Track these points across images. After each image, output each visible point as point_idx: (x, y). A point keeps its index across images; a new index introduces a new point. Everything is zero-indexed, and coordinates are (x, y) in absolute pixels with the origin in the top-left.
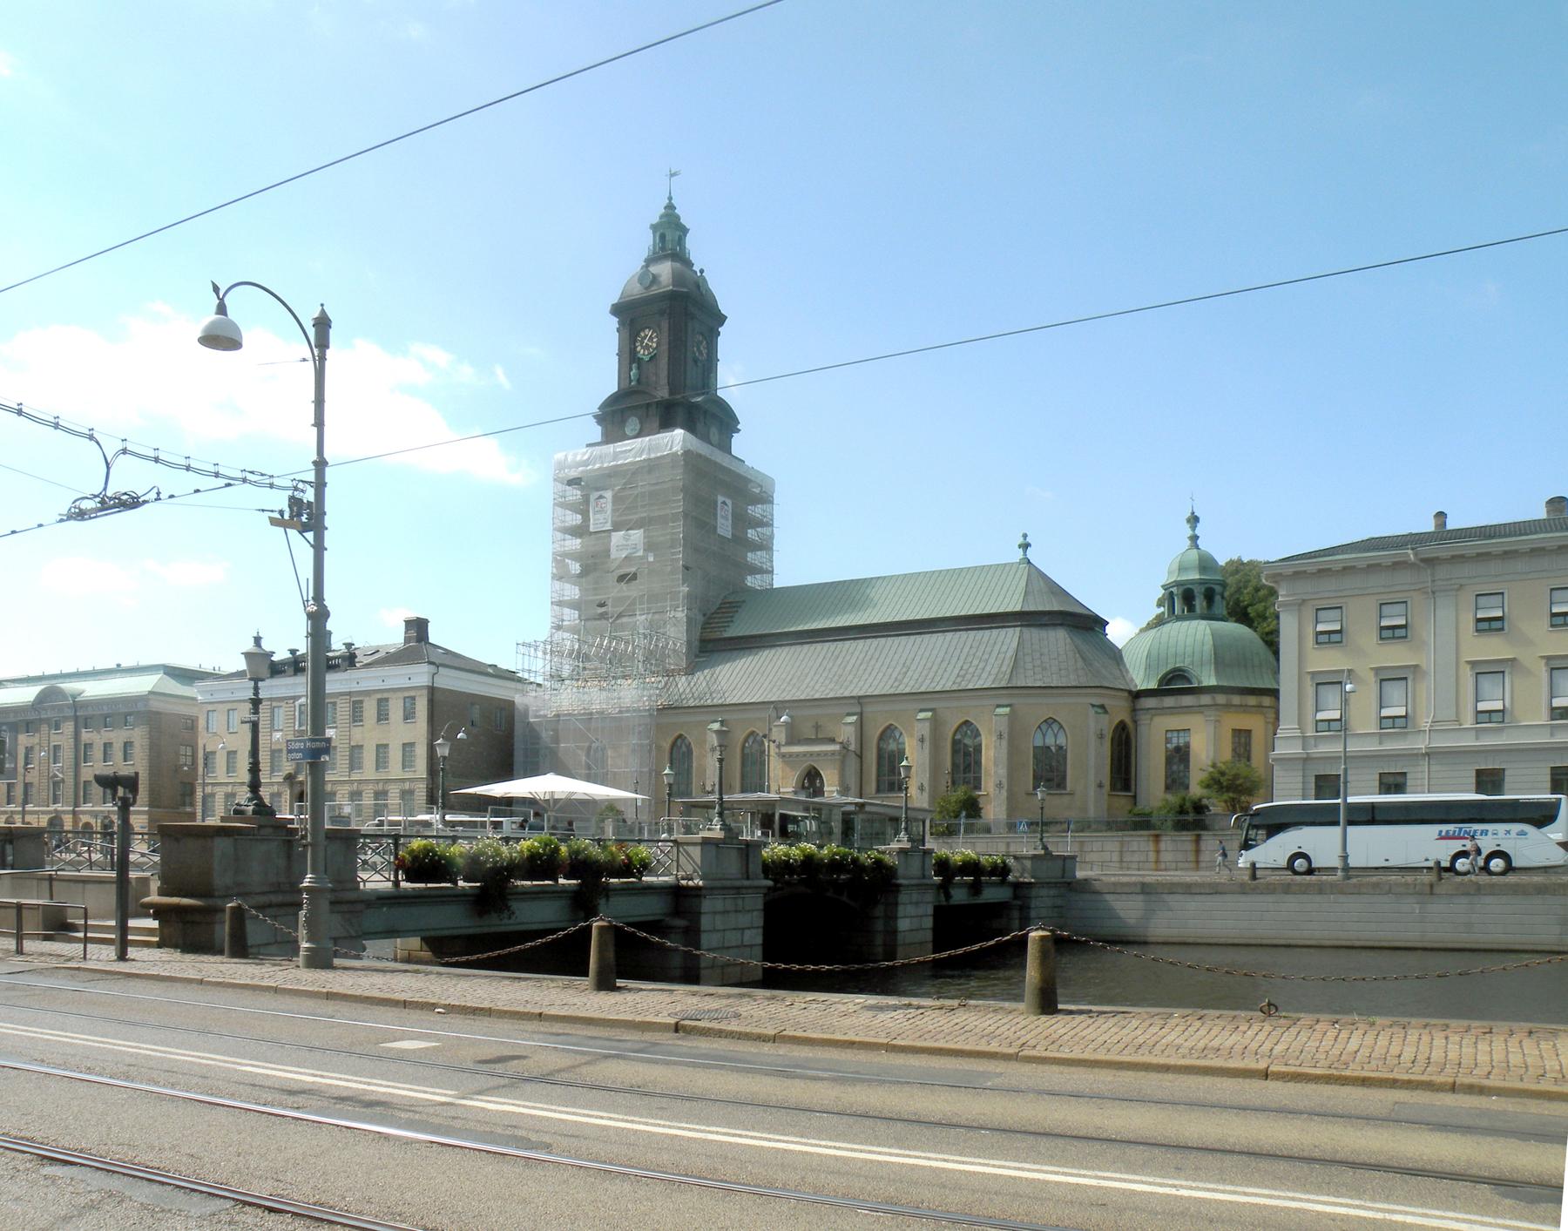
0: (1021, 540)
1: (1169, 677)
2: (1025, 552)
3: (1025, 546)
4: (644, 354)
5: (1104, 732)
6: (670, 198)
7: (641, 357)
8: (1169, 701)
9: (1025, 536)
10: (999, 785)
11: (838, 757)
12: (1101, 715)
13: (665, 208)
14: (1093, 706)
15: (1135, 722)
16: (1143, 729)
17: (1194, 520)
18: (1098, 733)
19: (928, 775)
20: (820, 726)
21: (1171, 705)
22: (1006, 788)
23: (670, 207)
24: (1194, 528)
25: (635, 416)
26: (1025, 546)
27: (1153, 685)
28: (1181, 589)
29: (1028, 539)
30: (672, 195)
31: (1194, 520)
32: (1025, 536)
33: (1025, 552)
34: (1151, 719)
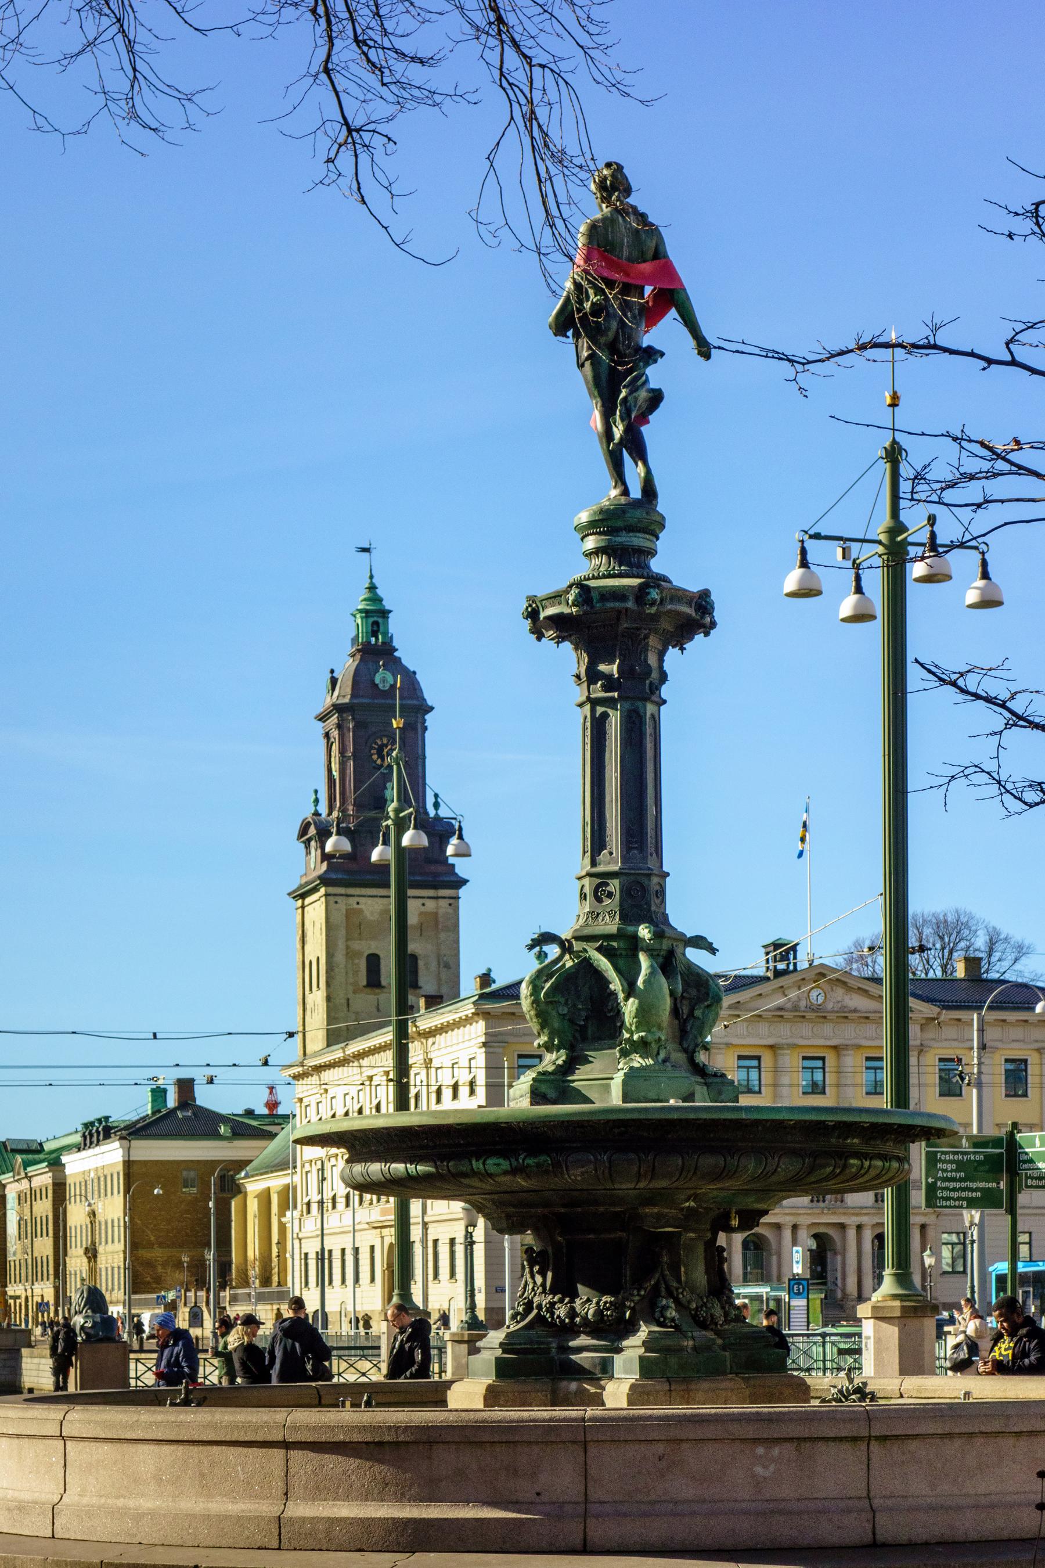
6: (371, 577)
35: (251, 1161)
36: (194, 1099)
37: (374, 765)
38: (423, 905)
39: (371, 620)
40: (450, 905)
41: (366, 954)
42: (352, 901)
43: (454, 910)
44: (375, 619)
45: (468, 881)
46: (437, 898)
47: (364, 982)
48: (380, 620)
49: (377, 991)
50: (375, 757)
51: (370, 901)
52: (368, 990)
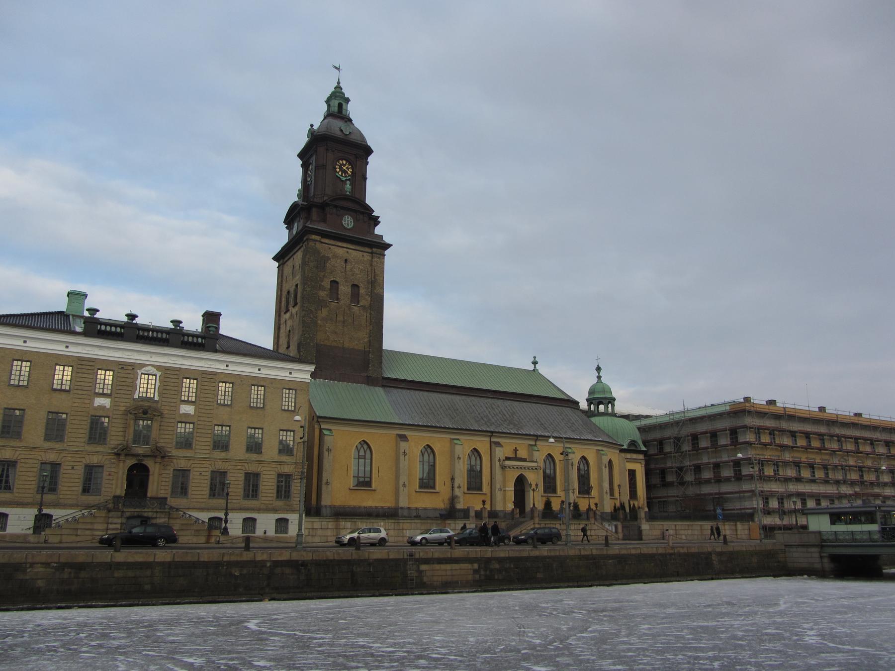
2: (535, 367)
3: (535, 363)
4: (342, 175)
6: (339, 83)
7: (339, 176)
13: (335, 88)
17: (598, 369)
20: (518, 450)
23: (338, 87)
24: (599, 373)
25: (352, 217)
26: (535, 363)
28: (608, 401)
29: (537, 359)
31: (598, 369)
32: (535, 358)
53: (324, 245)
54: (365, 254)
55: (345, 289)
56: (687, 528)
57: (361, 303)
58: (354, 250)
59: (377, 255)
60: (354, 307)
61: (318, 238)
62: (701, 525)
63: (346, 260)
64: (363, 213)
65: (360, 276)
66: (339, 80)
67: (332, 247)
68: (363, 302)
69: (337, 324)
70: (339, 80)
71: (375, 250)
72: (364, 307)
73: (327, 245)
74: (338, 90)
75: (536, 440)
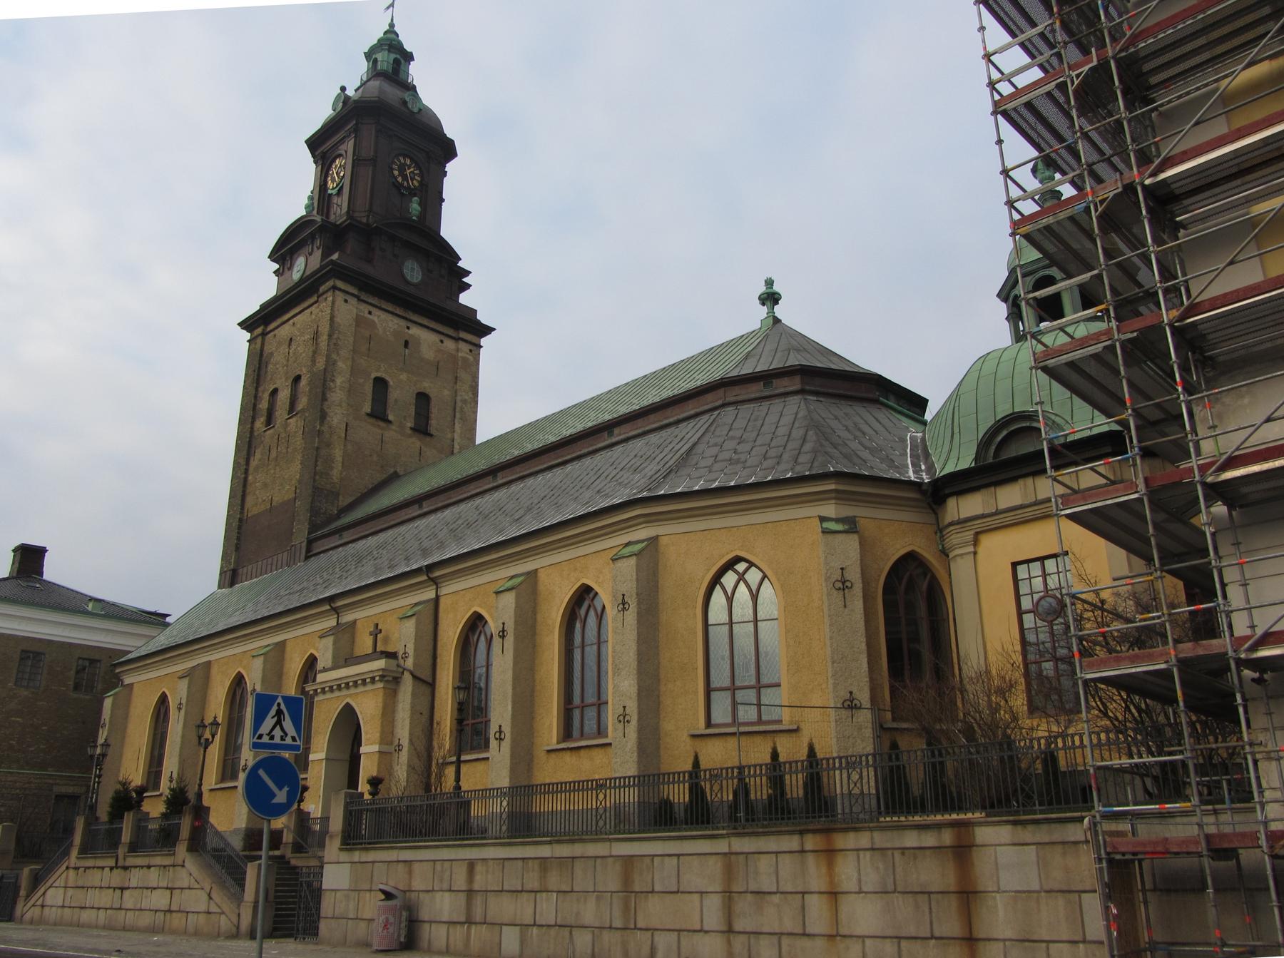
0: (762, 289)
1: (999, 438)
3: (770, 298)
5: (847, 576)
6: (392, 25)
8: (1010, 495)
9: (769, 283)
10: (623, 718)
11: (381, 685)
12: (841, 537)
14: (823, 519)
15: (944, 553)
16: (961, 569)
18: (837, 576)
19: (510, 708)
21: (1017, 501)
22: (634, 722)
26: (770, 298)
27: (966, 462)
29: (776, 288)
30: (394, 22)
32: (769, 283)
33: (771, 311)
34: (976, 542)
35: (130, 652)
36: (41, 574)
37: (394, 180)
38: (442, 341)
39: (393, 56)
40: (471, 351)
41: (373, 376)
42: (365, 308)
43: (474, 358)
44: (398, 56)
45: (495, 329)
46: (457, 339)
47: (367, 408)
48: (403, 61)
49: (382, 424)
50: (396, 173)
51: (384, 316)
52: (372, 420)
53: (270, 335)
54: (313, 308)
55: (284, 395)
56: (532, 881)
57: (300, 407)
58: (300, 312)
59: (324, 296)
60: (291, 420)
61: (259, 331)
62: (628, 862)
63: (291, 339)
64: (312, 237)
65: (304, 355)
66: (392, 20)
67: (276, 332)
68: (302, 402)
69: (270, 467)
70: (392, 20)
71: (322, 289)
72: (303, 410)
73: (272, 333)
74: (389, 36)
75: (435, 582)
